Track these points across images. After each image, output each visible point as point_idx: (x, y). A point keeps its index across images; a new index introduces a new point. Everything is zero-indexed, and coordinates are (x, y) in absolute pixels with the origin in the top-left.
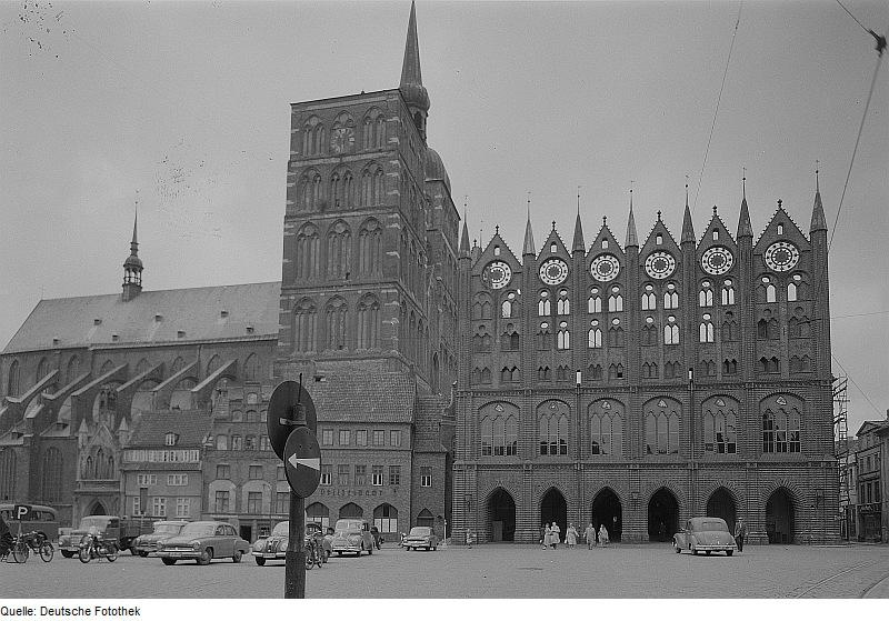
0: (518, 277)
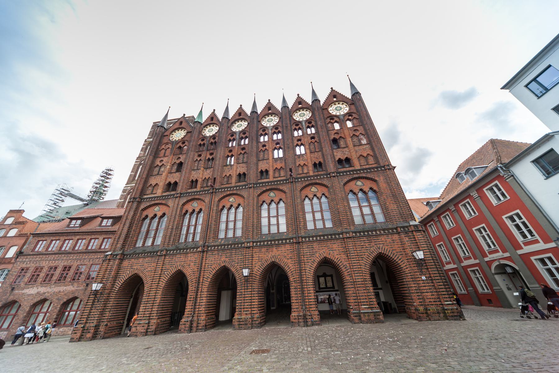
0: (189, 134)
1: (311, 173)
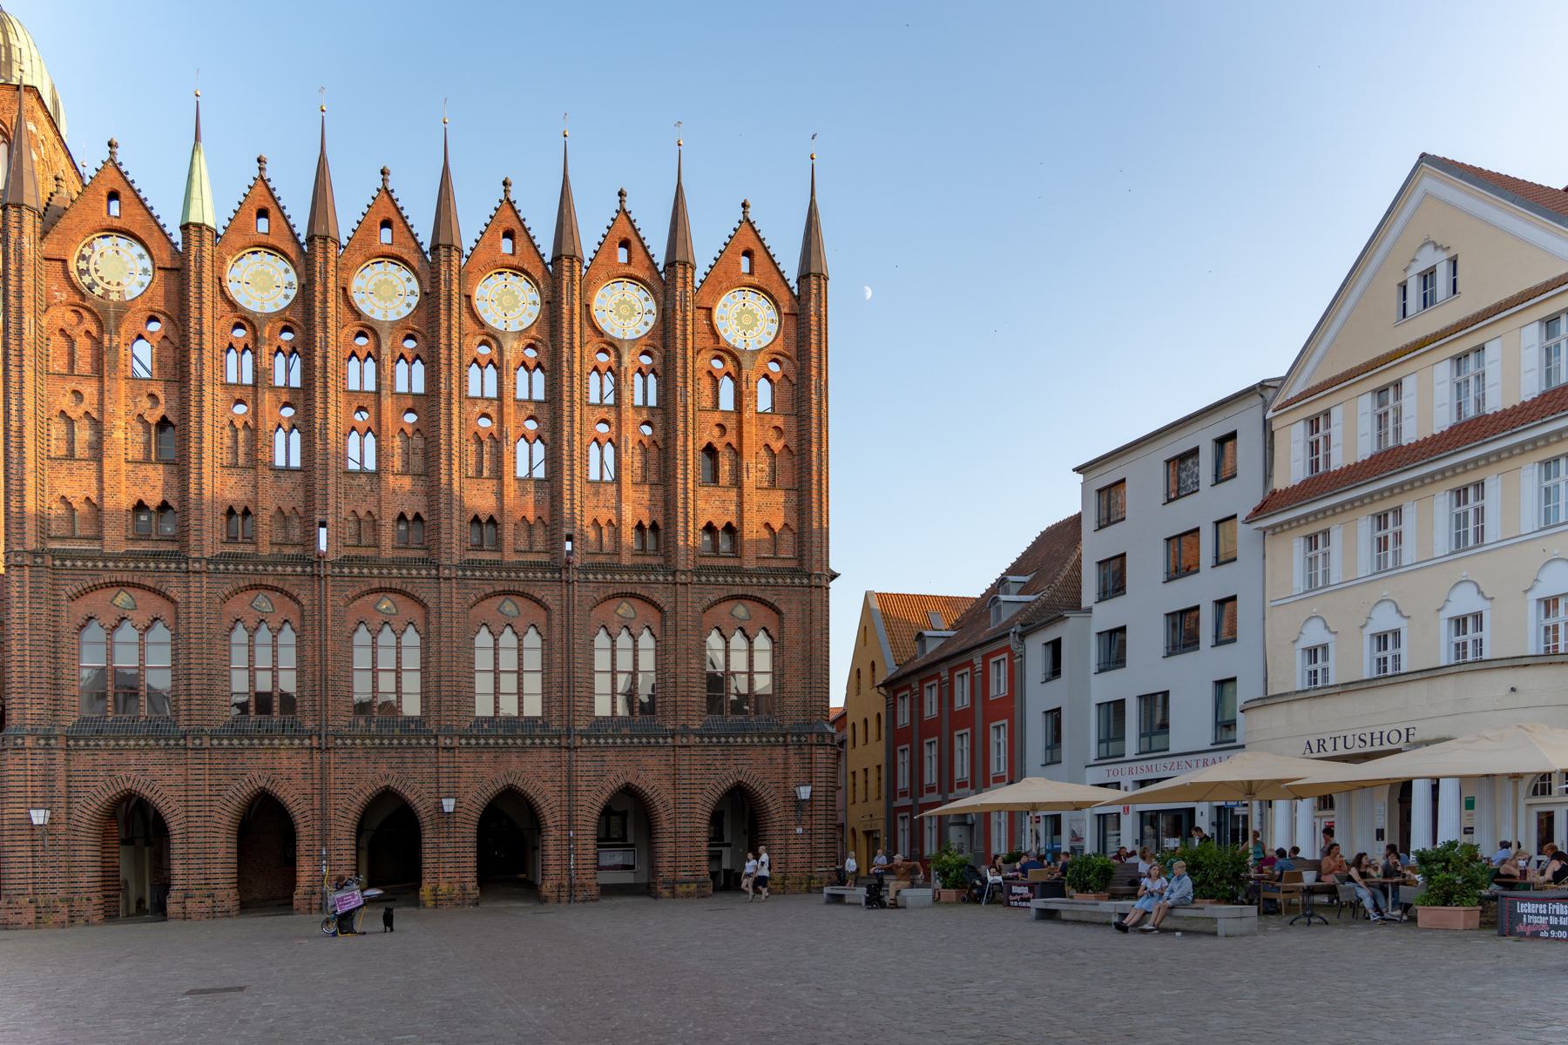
1: (626, 560)
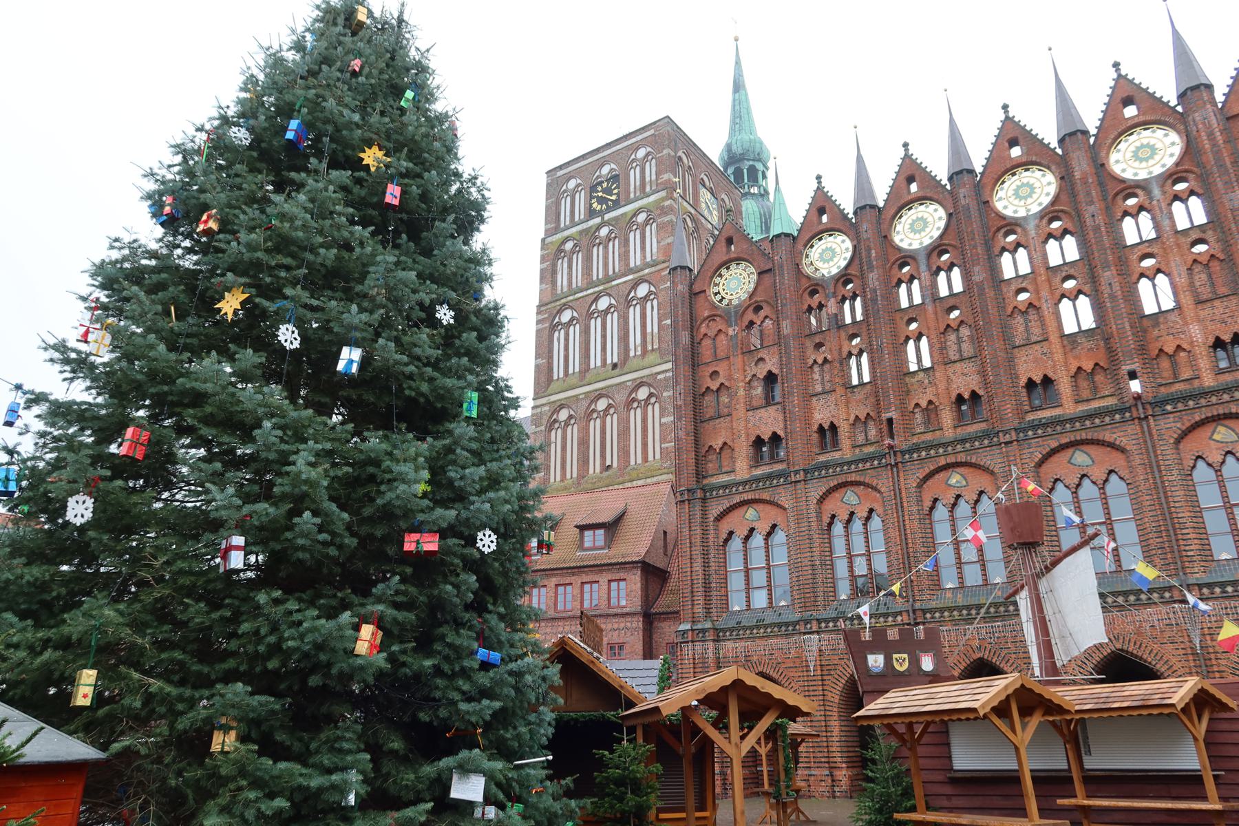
1: (1209, 381)
